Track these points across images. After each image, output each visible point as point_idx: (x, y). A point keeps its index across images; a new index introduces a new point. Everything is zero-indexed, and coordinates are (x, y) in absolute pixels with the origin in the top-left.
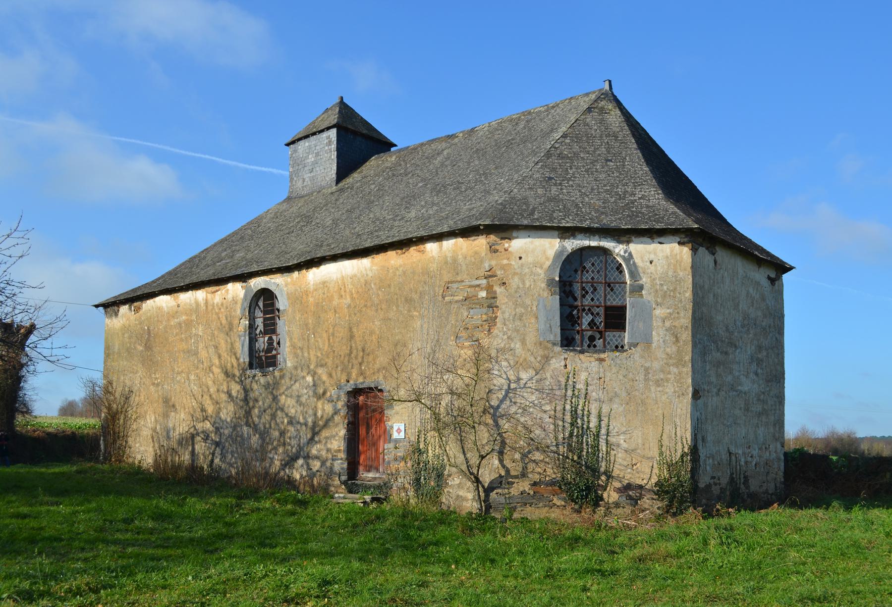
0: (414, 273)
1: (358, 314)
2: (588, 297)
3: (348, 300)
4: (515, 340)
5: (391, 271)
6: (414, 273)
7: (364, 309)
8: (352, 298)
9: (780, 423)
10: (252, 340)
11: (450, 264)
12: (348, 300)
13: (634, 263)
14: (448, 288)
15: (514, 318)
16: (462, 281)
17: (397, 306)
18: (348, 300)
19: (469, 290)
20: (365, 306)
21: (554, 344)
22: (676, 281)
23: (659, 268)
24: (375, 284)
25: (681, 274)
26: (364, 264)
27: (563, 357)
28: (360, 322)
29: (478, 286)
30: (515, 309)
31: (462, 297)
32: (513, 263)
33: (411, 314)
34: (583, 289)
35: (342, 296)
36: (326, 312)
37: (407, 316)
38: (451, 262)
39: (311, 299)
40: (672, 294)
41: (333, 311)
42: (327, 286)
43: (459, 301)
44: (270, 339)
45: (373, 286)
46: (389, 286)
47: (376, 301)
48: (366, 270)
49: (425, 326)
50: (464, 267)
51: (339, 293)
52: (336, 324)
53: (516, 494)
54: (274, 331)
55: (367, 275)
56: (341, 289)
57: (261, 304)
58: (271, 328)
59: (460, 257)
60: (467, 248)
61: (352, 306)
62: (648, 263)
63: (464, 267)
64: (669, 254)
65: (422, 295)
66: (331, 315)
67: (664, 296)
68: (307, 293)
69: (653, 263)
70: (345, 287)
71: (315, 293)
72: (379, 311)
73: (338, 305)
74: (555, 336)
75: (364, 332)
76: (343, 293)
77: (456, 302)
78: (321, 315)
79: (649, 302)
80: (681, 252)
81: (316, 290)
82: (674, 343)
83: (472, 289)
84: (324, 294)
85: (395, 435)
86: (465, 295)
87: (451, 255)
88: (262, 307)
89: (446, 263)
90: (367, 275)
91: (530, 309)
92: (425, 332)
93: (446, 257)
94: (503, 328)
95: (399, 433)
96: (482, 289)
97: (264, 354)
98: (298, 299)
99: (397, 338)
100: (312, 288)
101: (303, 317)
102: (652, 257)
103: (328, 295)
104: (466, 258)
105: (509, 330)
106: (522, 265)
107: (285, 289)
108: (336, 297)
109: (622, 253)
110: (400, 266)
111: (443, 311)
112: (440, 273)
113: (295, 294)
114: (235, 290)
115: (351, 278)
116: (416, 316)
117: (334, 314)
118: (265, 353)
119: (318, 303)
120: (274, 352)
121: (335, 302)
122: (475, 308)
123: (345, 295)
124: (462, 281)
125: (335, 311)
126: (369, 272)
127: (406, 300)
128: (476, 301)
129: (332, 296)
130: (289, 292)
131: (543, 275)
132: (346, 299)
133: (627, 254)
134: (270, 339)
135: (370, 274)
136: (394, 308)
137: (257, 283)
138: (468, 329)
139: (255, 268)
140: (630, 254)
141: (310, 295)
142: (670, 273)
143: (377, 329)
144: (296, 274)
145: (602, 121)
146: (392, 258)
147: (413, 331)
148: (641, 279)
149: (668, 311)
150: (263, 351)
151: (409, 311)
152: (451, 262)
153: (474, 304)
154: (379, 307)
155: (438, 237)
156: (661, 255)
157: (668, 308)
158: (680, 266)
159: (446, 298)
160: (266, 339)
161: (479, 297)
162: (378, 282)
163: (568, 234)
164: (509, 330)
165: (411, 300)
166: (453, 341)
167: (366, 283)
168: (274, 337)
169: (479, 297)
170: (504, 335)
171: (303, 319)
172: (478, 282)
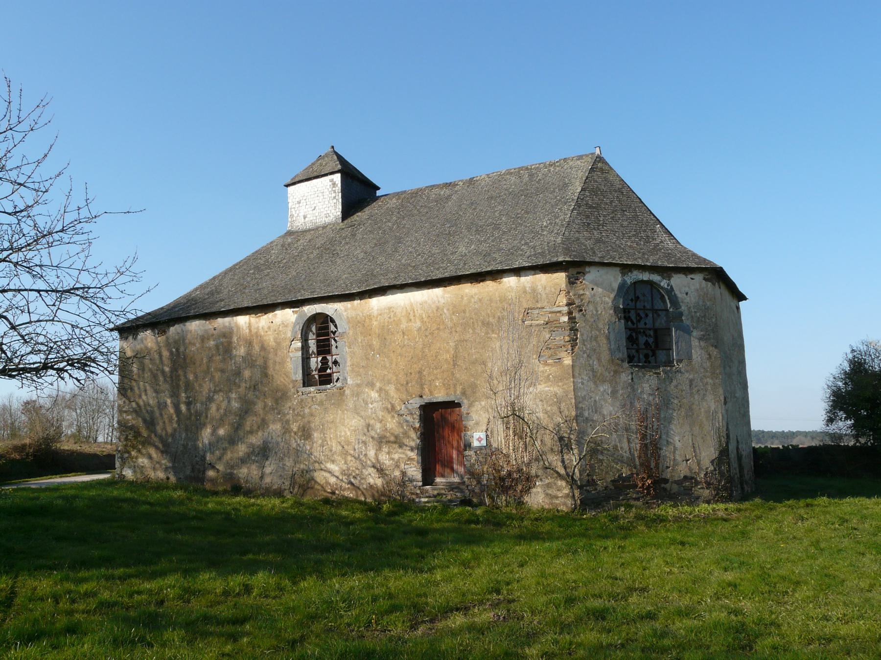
0: (491, 300)
1: (430, 337)
2: (642, 322)
3: (419, 324)
4: (592, 357)
5: (465, 299)
6: (491, 300)
7: (436, 332)
8: (423, 322)
9: (748, 423)
10: (306, 359)
11: (530, 293)
12: (418, 324)
13: (675, 293)
14: (527, 314)
15: (591, 339)
16: (543, 308)
17: (474, 329)
18: (418, 324)
19: (550, 315)
20: (438, 329)
21: (623, 361)
22: (705, 309)
23: (692, 299)
24: (448, 310)
25: (708, 303)
26: (438, 292)
27: (629, 372)
28: (432, 343)
29: (560, 312)
30: (591, 332)
31: (543, 322)
32: (587, 293)
33: (489, 336)
34: (638, 315)
35: (411, 320)
36: (393, 334)
37: (484, 337)
38: (530, 291)
39: (375, 323)
40: (703, 319)
41: (401, 333)
42: (393, 311)
43: (541, 325)
44: (324, 359)
45: (445, 311)
46: (464, 311)
47: (450, 324)
48: (437, 297)
49: (505, 347)
50: (544, 296)
51: (408, 317)
52: (405, 345)
53: (601, 489)
54: (329, 352)
55: (439, 302)
56: (410, 314)
57: (314, 329)
58: (324, 348)
59: (539, 287)
60: (546, 280)
61: (423, 329)
62: (685, 295)
63: (544, 296)
64: (698, 287)
65: (500, 320)
66: (398, 337)
67: (698, 321)
68: (370, 317)
69: (688, 295)
70: (414, 312)
71: (379, 317)
72: (454, 333)
73: (406, 328)
74: (623, 354)
75: (437, 352)
76: (412, 318)
77: (537, 325)
78: (387, 337)
79: (688, 325)
80: (707, 286)
81: (381, 315)
82: (708, 359)
83: (553, 315)
84: (390, 318)
85: (476, 444)
86: (547, 320)
87: (530, 286)
88: (314, 331)
89: (525, 292)
90: (439, 302)
91: (602, 332)
92: (505, 351)
93: (525, 288)
94: (583, 348)
95: (480, 441)
96: (563, 315)
97: (317, 372)
98: (362, 324)
99: (474, 357)
100: (375, 313)
101: (365, 339)
102: (687, 289)
103: (395, 319)
104: (545, 288)
105: (588, 349)
106: (594, 295)
107: (345, 314)
108: (404, 321)
109: (666, 286)
110: (476, 294)
111: (524, 334)
112: (519, 301)
113: (356, 318)
114: (288, 316)
115: (420, 304)
116: (495, 338)
117: (402, 336)
118: (319, 372)
119: (383, 326)
120: (329, 371)
121: (403, 326)
122: (557, 331)
123: (415, 319)
124: (543, 308)
125: (403, 333)
126: (440, 300)
127: (483, 323)
128: (559, 325)
129: (400, 320)
130: (349, 316)
131: (610, 304)
132: (415, 322)
133: (669, 288)
134: (324, 359)
135: (442, 301)
136: (471, 331)
137: (310, 310)
138: (550, 349)
139: (308, 296)
140: (672, 287)
141: (374, 319)
142: (701, 303)
143: (451, 349)
144: (357, 302)
145: (606, 179)
146: (468, 289)
147: (492, 351)
148: (681, 307)
149: (702, 333)
150: (315, 370)
151: (487, 333)
152: (530, 291)
153: (556, 327)
154: (453, 329)
155: (517, 272)
156: (693, 288)
157: (702, 331)
158: (707, 297)
159: (525, 323)
160: (320, 359)
161: (561, 321)
162: (451, 308)
163: (626, 270)
164: (588, 349)
165: (488, 324)
166: (536, 359)
167: (438, 308)
168: (329, 357)
169: (561, 321)
170: (584, 353)
171: (366, 341)
172: (559, 309)
